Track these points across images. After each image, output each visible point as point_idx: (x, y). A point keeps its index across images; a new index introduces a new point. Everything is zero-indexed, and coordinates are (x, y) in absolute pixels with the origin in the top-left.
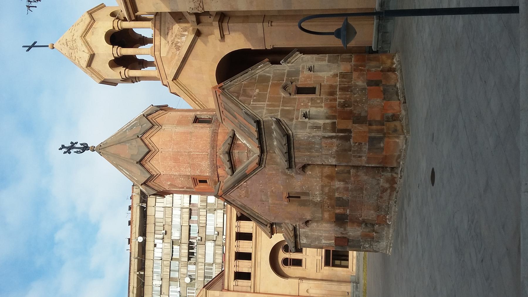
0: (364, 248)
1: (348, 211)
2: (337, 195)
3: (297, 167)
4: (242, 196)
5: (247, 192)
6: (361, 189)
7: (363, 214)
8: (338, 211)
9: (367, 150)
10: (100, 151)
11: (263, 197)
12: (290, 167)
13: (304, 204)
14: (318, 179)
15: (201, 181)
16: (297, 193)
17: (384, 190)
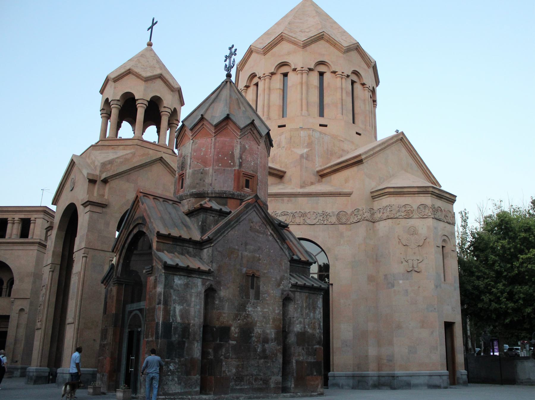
0: (168, 364)
1: (234, 342)
2: (258, 330)
3: (290, 292)
4: (252, 224)
5: (258, 231)
6: (265, 357)
7: (230, 360)
8: (233, 328)
9: (309, 361)
10: (228, 83)
11: (252, 247)
12: (295, 286)
13: (244, 292)
14: (277, 312)
15: (247, 182)
16: (258, 287)
17: (266, 382)
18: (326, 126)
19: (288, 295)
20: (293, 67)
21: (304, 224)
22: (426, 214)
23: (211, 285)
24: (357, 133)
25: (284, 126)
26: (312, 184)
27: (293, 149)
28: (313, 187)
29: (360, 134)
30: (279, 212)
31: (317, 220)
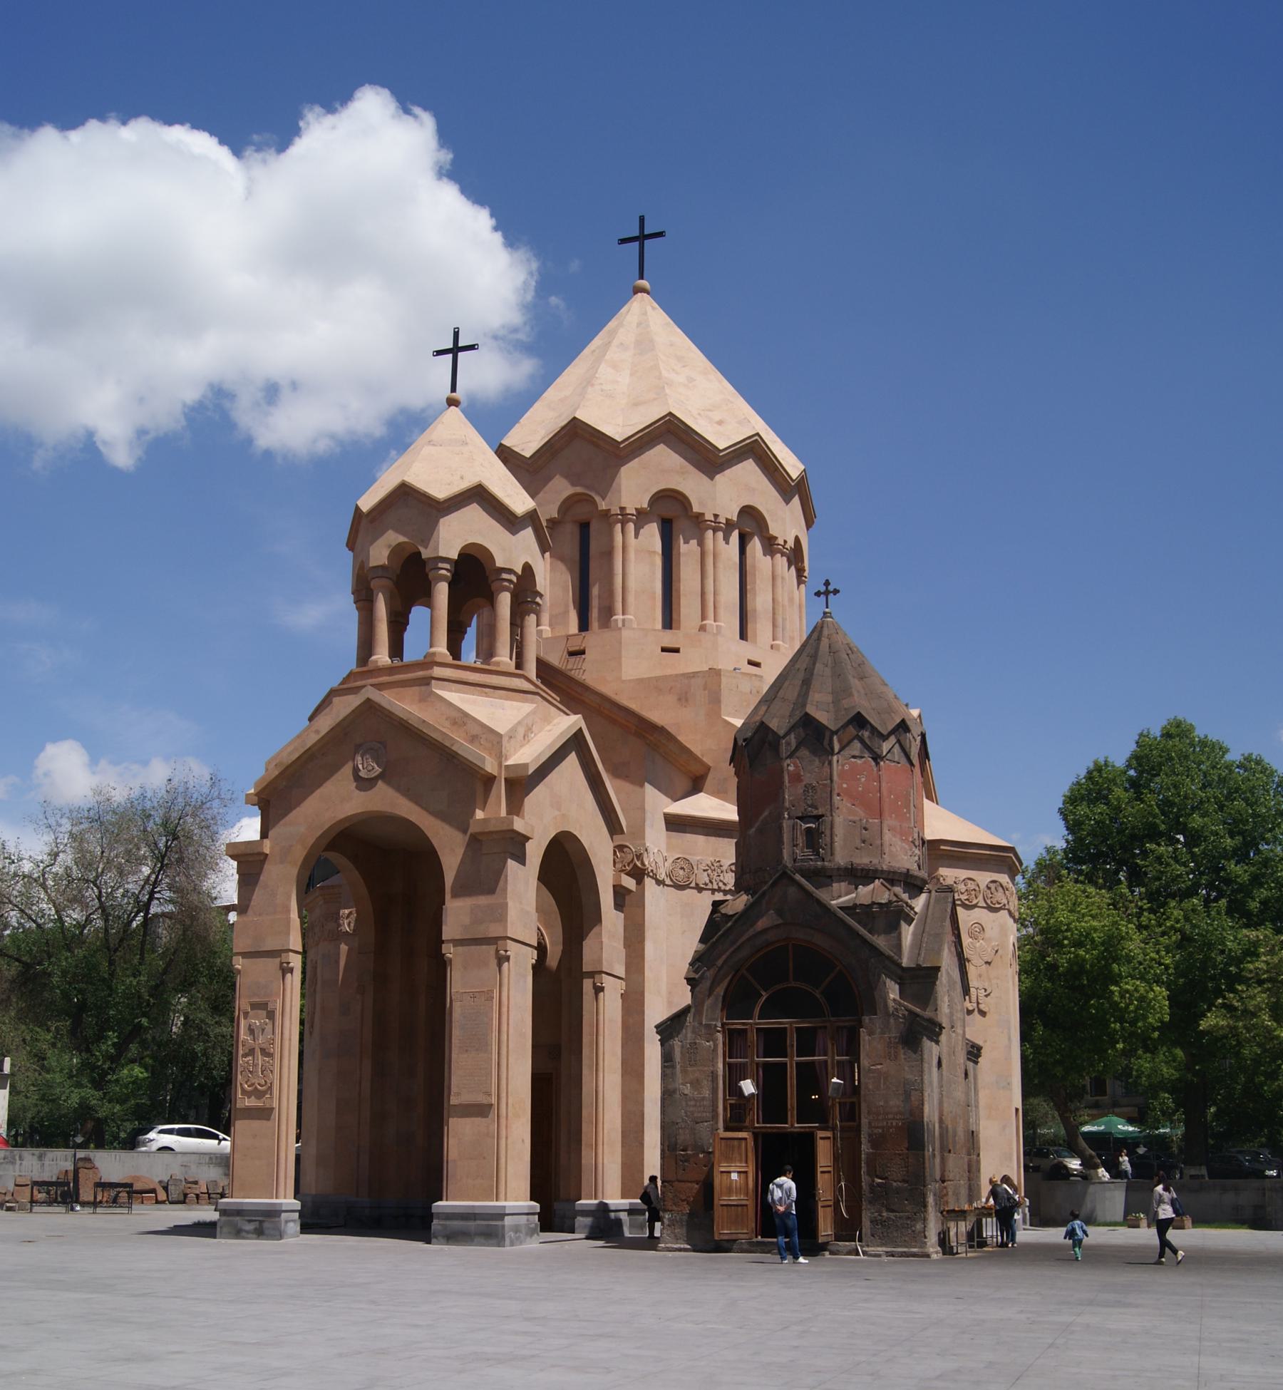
20: (696, 509)
25: (677, 650)
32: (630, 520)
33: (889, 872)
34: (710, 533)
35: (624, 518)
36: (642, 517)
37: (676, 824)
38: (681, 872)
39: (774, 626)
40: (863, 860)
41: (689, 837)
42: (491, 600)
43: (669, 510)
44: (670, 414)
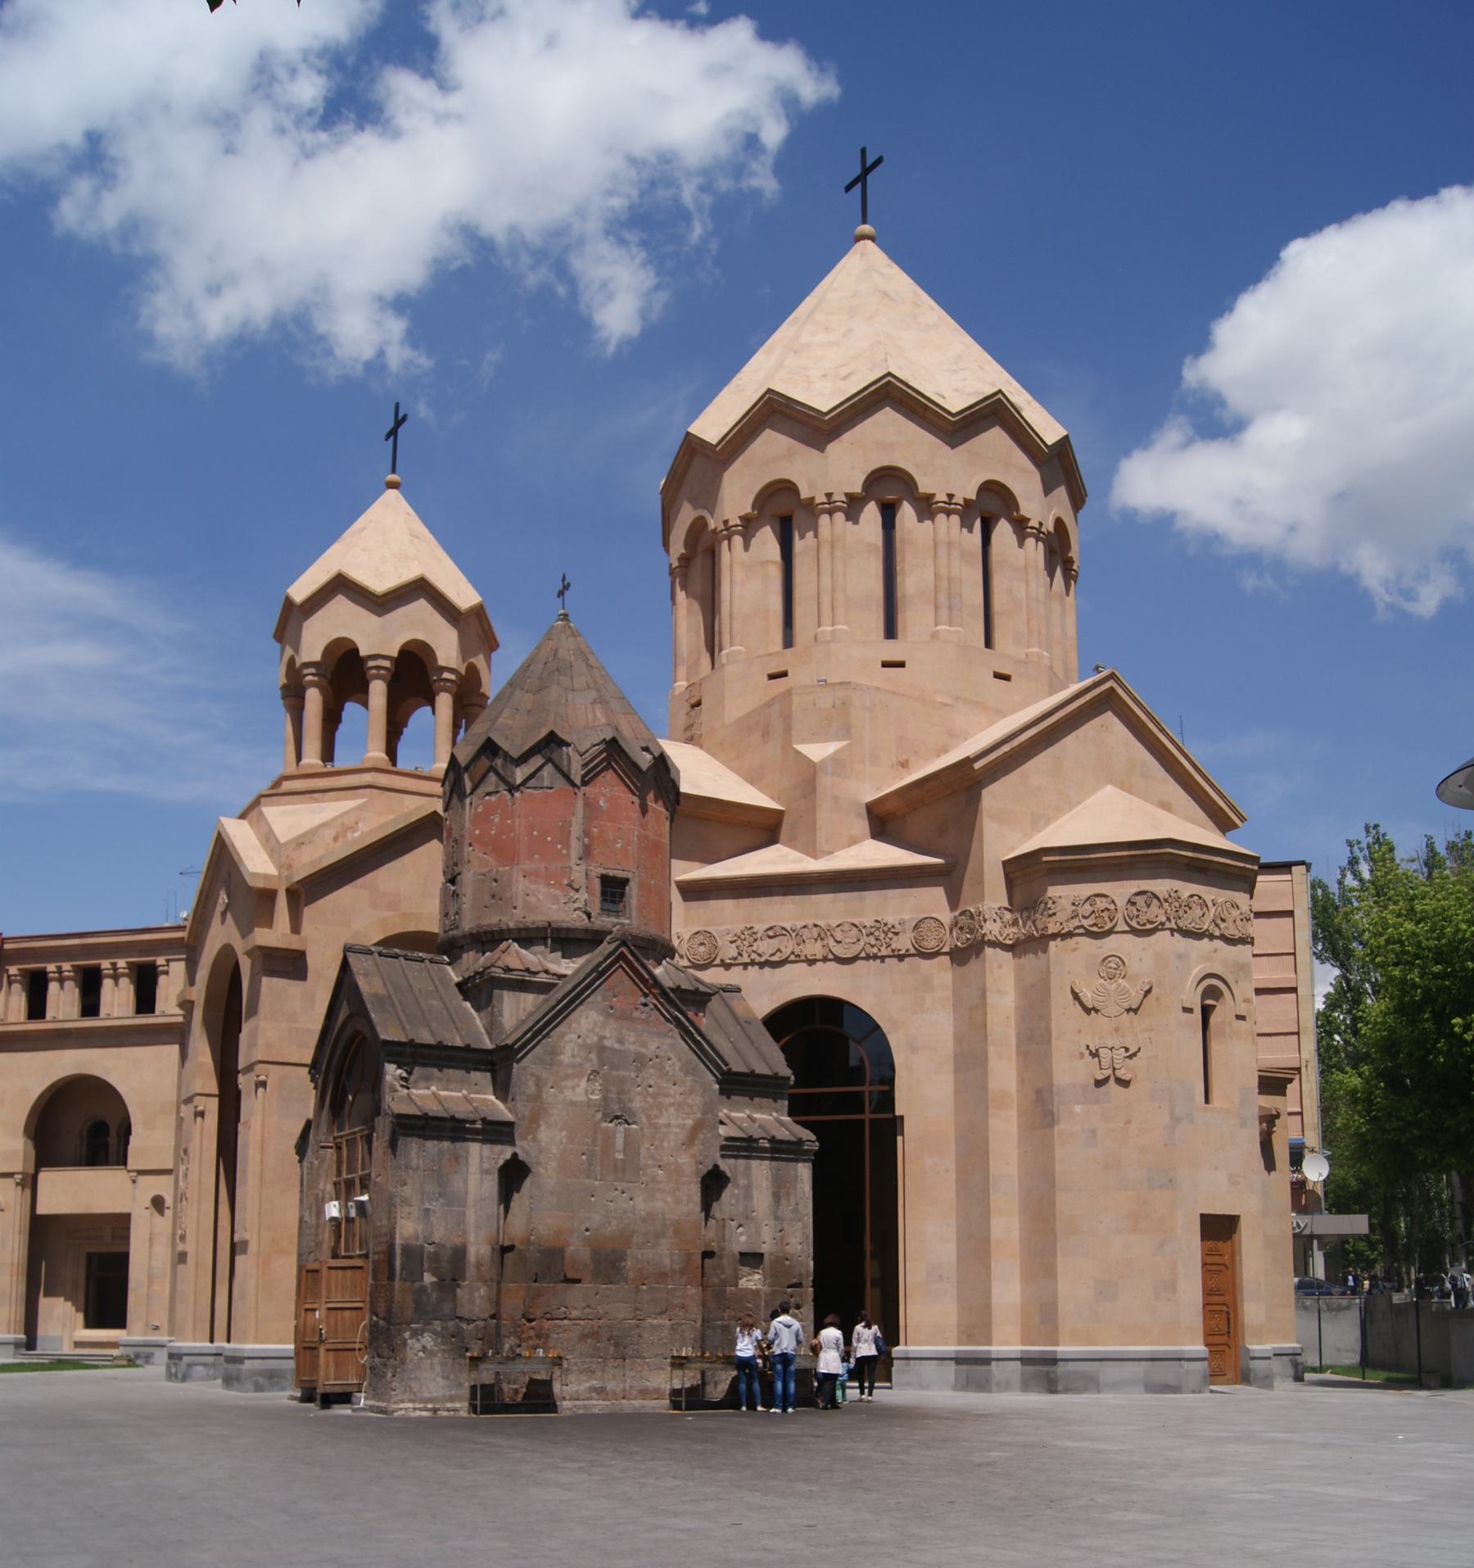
18: (901, 665)
19: (716, 1166)
21: (825, 959)
22: (1151, 917)
23: (515, 1155)
24: (997, 676)
25: (784, 674)
26: (854, 841)
27: (798, 747)
28: (854, 850)
29: (1007, 678)
30: (760, 928)
31: (862, 943)
32: (736, 533)
33: (519, 930)
34: (824, 519)
35: (729, 531)
36: (748, 527)
37: (695, 891)
38: (702, 949)
39: (936, 608)
40: (492, 920)
41: (714, 904)
42: (365, 690)
43: (781, 506)
44: (769, 391)
